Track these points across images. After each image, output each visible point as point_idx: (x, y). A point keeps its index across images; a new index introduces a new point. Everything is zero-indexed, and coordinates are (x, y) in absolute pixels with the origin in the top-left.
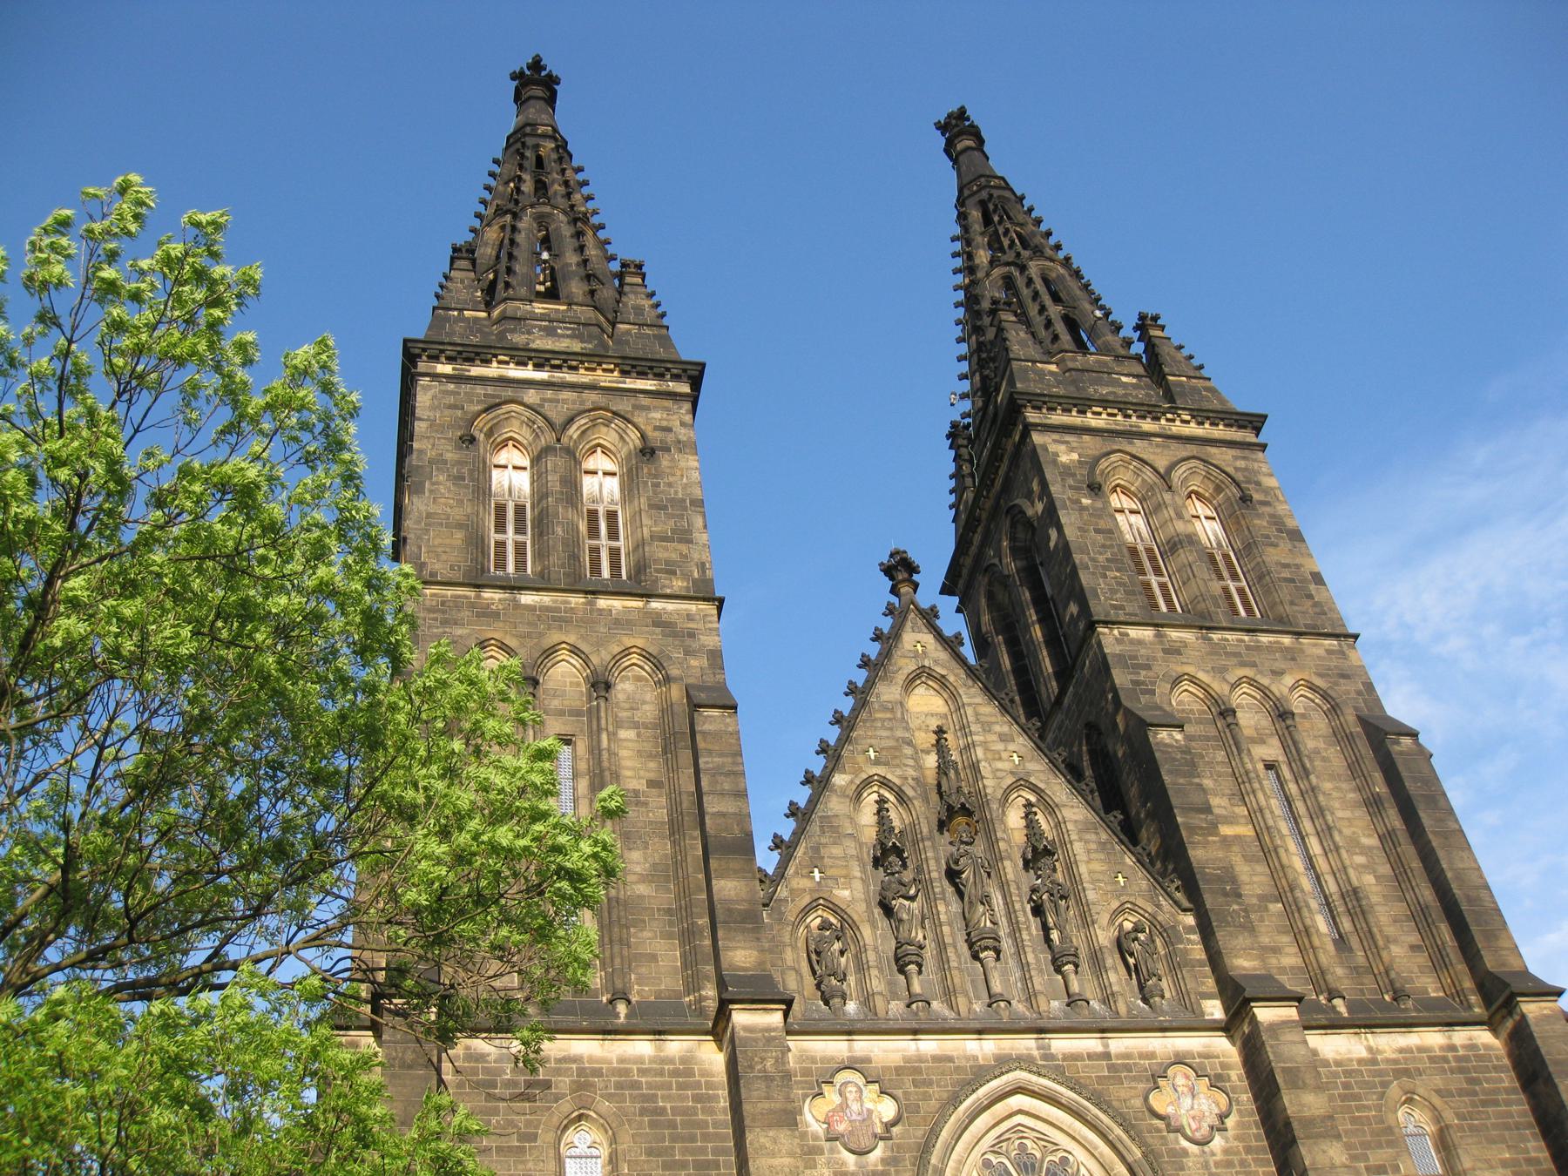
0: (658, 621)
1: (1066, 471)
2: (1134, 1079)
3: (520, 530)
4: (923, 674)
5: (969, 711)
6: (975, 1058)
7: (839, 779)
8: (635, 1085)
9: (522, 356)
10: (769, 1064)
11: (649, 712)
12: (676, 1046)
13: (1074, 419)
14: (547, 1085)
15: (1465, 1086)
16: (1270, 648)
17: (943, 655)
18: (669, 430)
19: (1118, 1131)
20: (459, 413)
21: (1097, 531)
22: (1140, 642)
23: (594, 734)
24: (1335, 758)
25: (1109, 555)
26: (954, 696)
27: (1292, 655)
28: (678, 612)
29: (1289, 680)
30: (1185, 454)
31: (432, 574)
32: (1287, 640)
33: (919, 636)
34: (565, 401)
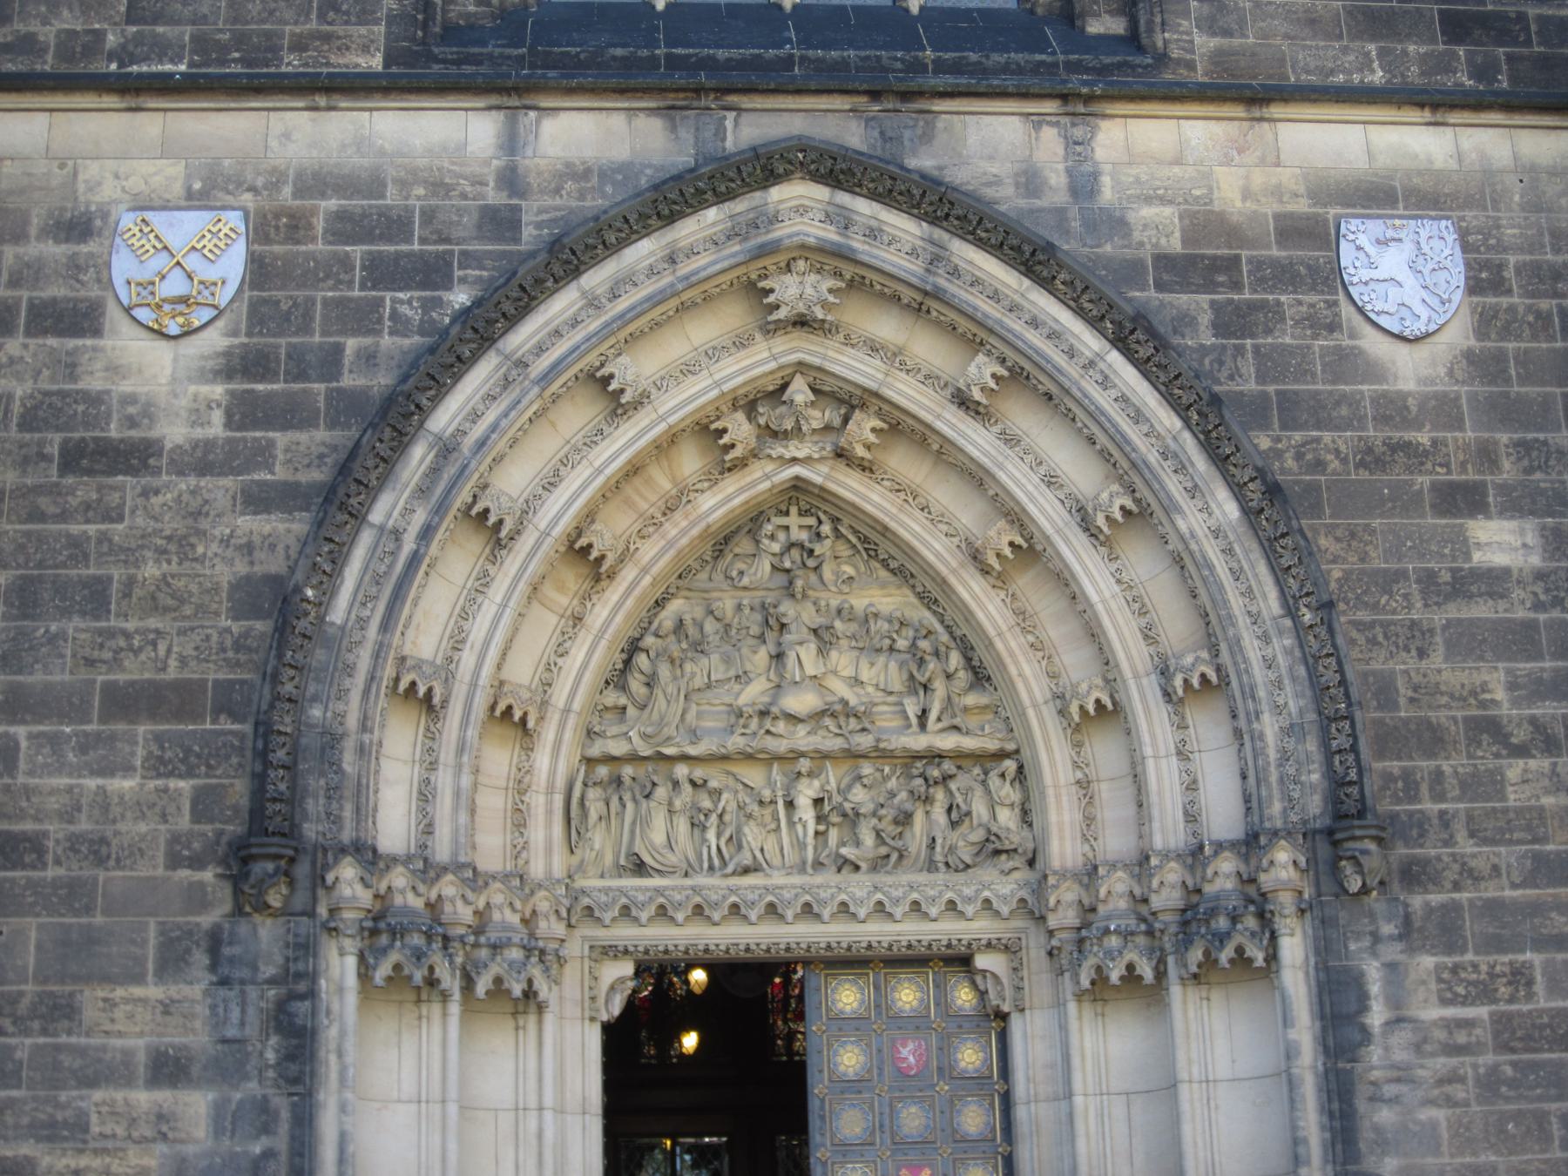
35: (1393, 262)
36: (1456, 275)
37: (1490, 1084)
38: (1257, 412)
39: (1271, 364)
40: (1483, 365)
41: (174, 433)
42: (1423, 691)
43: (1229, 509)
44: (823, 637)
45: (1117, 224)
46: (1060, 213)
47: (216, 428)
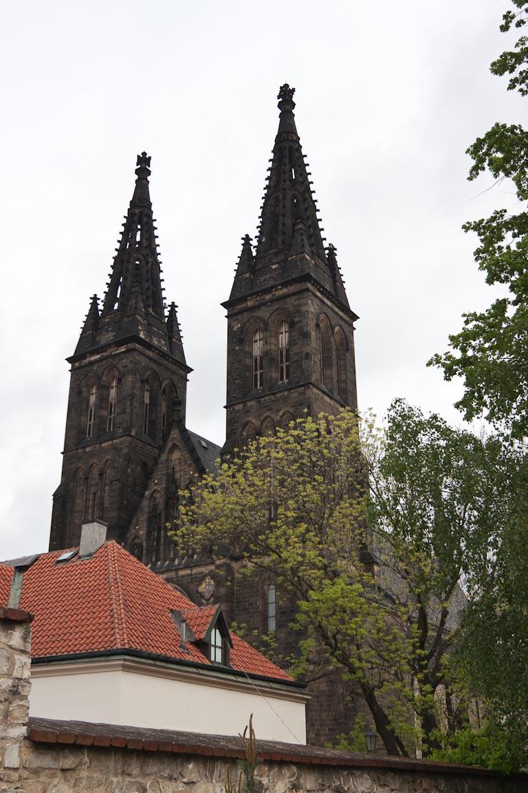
13: (243, 306)
18: (126, 366)
22: (238, 411)
25: (238, 373)
32: (286, 393)
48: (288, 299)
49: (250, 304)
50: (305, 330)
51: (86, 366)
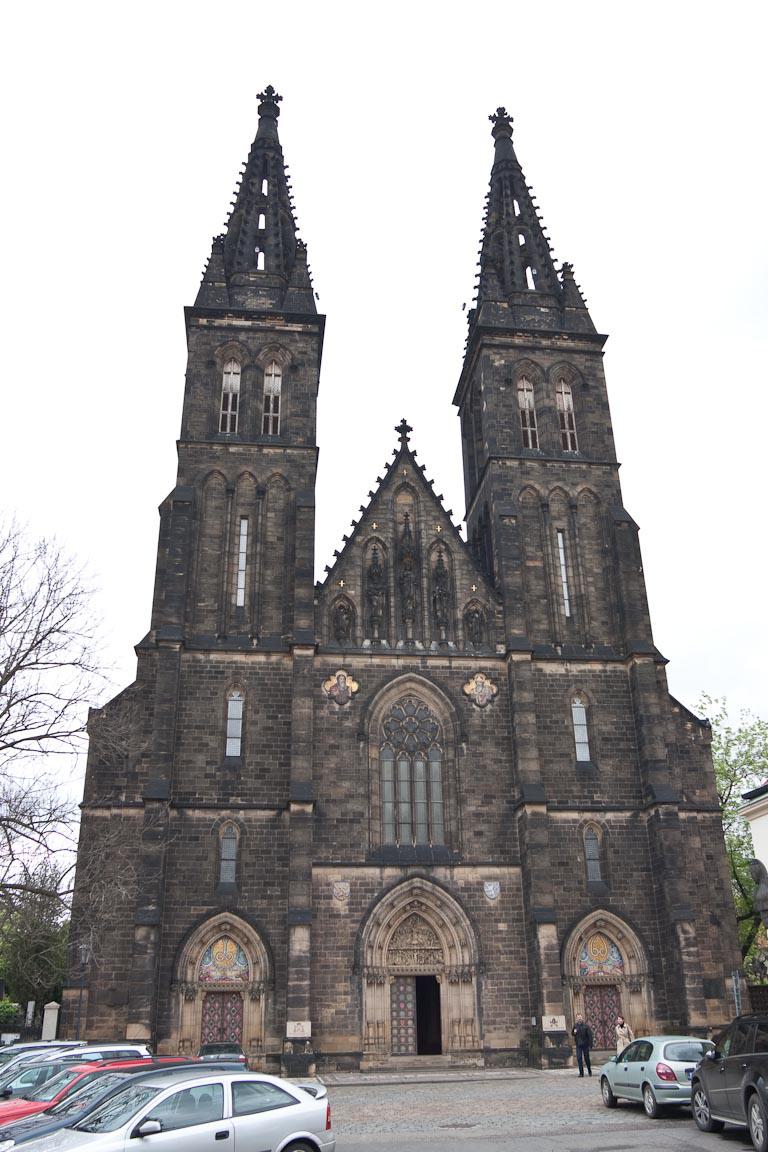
0: (290, 460)
1: (497, 370)
2: (460, 678)
3: (234, 409)
4: (405, 486)
5: (422, 505)
6: (394, 666)
7: (359, 539)
8: (257, 673)
9: (238, 315)
10: (305, 671)
11: (281, 504)
12: (274, 658)
13: (508, 340)
14: (223, 672)
15: (605, 688)
16: (575, 471)
17: (415, 476)
18: (305, 353)
19: (448, 700)
20: (208, 347)
21: (504, 406)
23: (256, 517)
24: (592, 526)
26: (416, 497)
27: (584, 475)
28: (298, 455)
29: (579, 488)
30: (561, 358)
31: (192, 437)
32: (584, 467)
33: (406, 466)
34: (258, 338)
35: (491, 888)
36: (499, 890)
37: (496, 997)
38: (472, 909)
39: (475, 902)
40: (501, 902)
41: (342, 913)
42: (491, 946)
43: (468, 922)
44: (418, 933)
45: (455, 883)
46: (449, 882)
47: (347, 912)
48: (576, 356)
49: (517, 341)
50: (604, 400)
51: (220, 328)
